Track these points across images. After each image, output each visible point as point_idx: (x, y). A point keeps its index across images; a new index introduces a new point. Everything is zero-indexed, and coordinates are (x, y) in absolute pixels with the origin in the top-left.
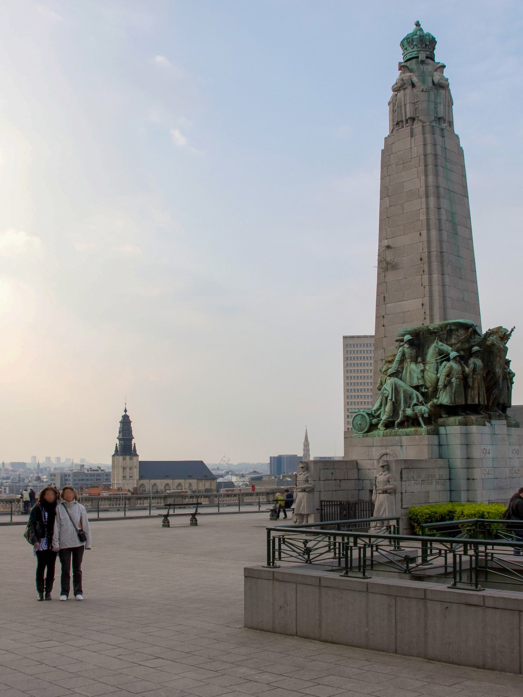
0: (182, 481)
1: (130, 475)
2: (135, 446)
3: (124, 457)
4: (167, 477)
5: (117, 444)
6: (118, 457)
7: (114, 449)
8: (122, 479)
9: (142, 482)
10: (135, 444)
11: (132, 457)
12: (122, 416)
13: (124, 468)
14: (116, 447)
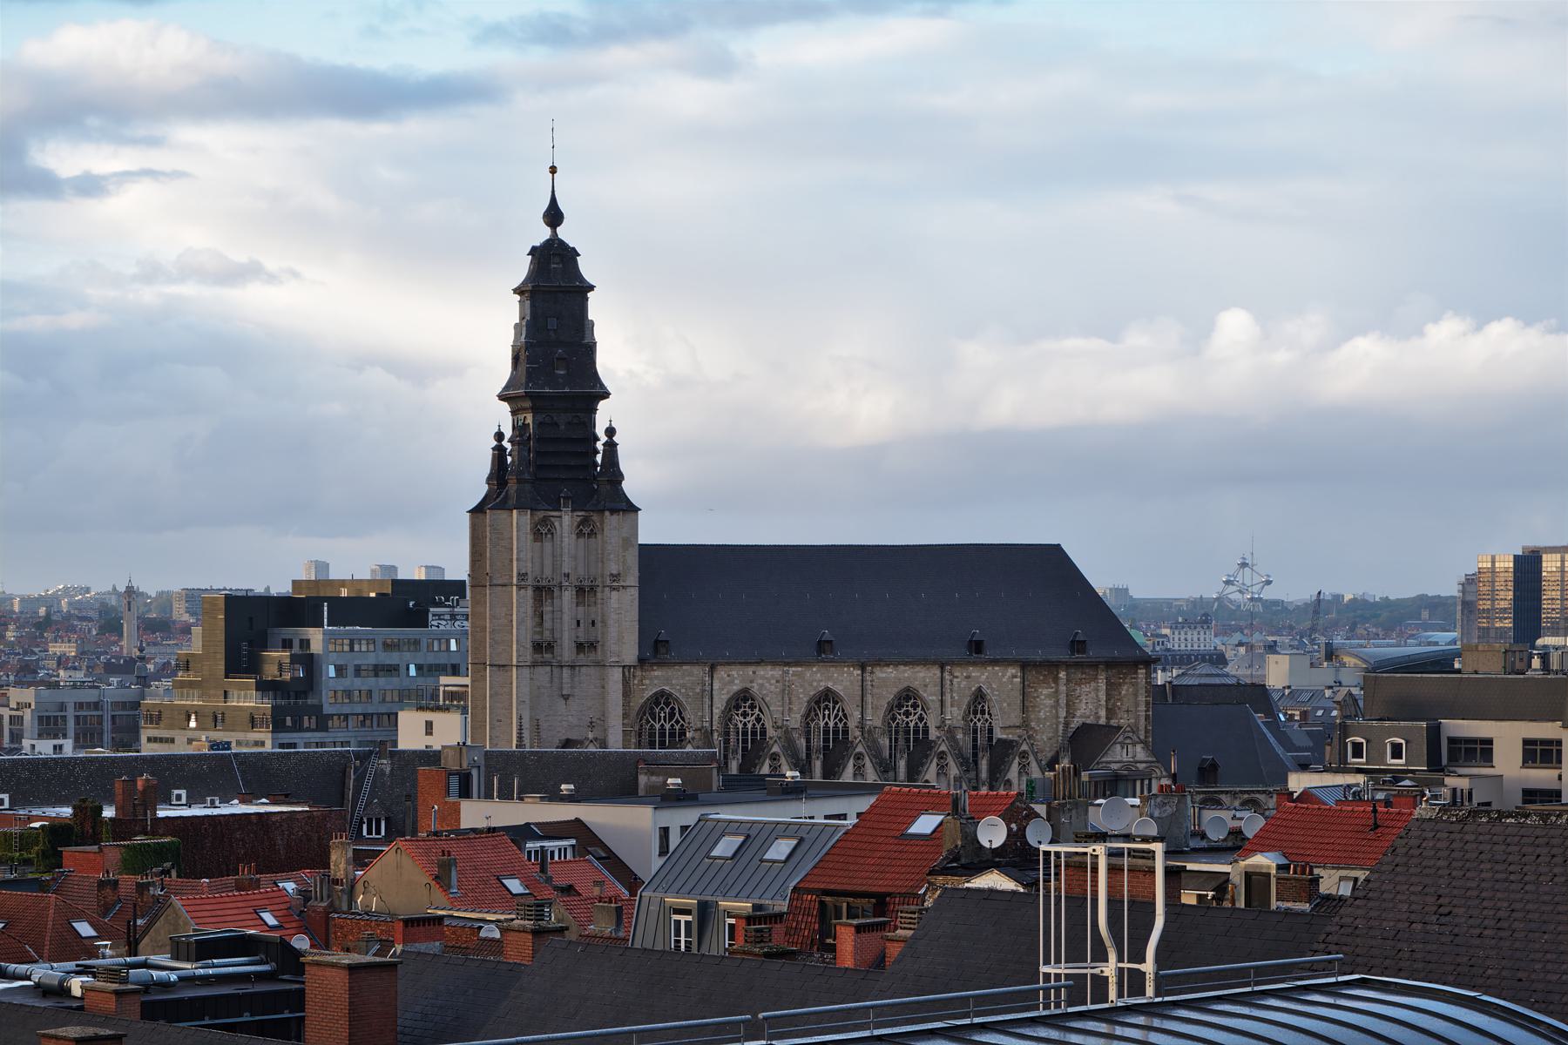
0: (922, 678)
1: (582, 640)
2: (611, 446)
3: (541, 514)
4: (823, 651)
6: (503, 515)
7: (485, 466)
8: (529, 657)
9: (657, 680)
10: (611, 432)
11: (595, 517)
12: (534, 251)
13: (543, 592)
14: (499, 451)
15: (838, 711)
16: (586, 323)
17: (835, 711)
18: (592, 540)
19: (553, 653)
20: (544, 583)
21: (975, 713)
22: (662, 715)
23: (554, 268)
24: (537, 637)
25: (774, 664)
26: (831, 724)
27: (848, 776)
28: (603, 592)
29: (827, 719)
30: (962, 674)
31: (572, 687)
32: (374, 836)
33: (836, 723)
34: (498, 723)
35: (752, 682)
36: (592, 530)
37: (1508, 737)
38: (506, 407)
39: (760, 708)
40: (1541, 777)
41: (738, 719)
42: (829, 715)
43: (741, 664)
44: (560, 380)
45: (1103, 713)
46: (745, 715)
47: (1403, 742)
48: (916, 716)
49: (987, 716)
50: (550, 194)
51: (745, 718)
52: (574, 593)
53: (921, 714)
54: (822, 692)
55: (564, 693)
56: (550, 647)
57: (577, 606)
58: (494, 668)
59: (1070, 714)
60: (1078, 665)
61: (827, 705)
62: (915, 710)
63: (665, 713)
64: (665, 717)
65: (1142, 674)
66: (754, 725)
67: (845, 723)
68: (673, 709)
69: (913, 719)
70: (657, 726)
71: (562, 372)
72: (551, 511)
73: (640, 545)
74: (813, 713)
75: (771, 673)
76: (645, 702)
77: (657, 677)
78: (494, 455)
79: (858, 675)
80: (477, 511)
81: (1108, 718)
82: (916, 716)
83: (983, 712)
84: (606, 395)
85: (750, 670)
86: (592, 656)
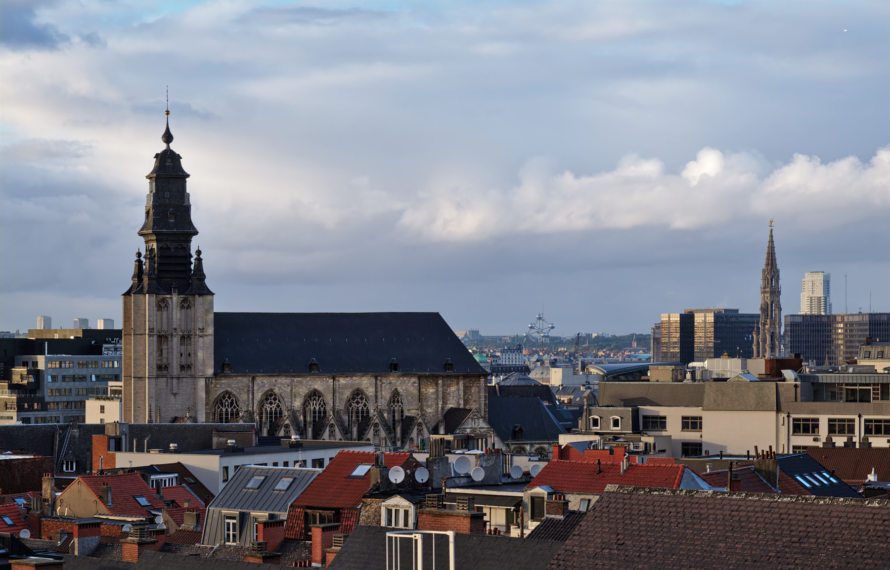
0: (366, 383)
1: (183, 363)
2: (199, 260)
3: (161, 297)
4: (311, 369)
5: (139, 254)
6: (141, 297)
7: (131, 269)
8: (155, 373)
10: (199, 252)
11: (190, 298)
12: (157, 156)
13: (162, 338)
14: (139, 262)
15: (321, 401)
16: (185, 194)
17: (319, 402)
18: (189, 310)
19: (168, 371)
20: (163, 333)
21: (394, 402)
22: (227, 403)
23: (168, 165)
24: (159, 362)
25: (286, 376)
26: (317, 408)
27: (326, 436)
28: (195, 338)
29: (315, 406)
30: (387, 382)
31: (178, 389)
32: (69, 471)
33: (320, 408)
34: (138, 409)
35: (274, 386)
36: (189, 305)
37: (673, 416)
38: (142, 239)
39: (279, 400)
40: (691, 436)
41: (268, 407)
42: (316, 403)
43: (269, 376)
44: (172, 225)
45: (462, 402)
46: (271, 403)
47: (619, 418)
48: (363, 404)
49: (400, 404)
50: (166, 125)
51: (271, 405)
52: (179, 338)
53: (365, 403)
54: (312, 391)
55: (174, 392)
56: (166, 367)
57: (181, 345)
58: (136, 379)
59: (445, 403)
60: (449, 377)
61: (315, 398)
62: (362, 400)
63: (228, 402)
64: (228, 405)
65: (482, 381)
66: (276, 409)
67: (325, 408)
68: (232, 400)
69: (361, 406)
70: (224, 410)
71: (172, 221)
72: (167, 294)
73: (217, 315)
74: (307, 403)
75: (284, 381)
76: (218, 397)
77: (224, 383)
78: (136, 265)
79: (331, 382)
80: (127, 294)
81: (465, 405)
82: (363, 404)
83: (398, 402)
84: (196, 233)
85: (274, 379)
86: (189, 373)
